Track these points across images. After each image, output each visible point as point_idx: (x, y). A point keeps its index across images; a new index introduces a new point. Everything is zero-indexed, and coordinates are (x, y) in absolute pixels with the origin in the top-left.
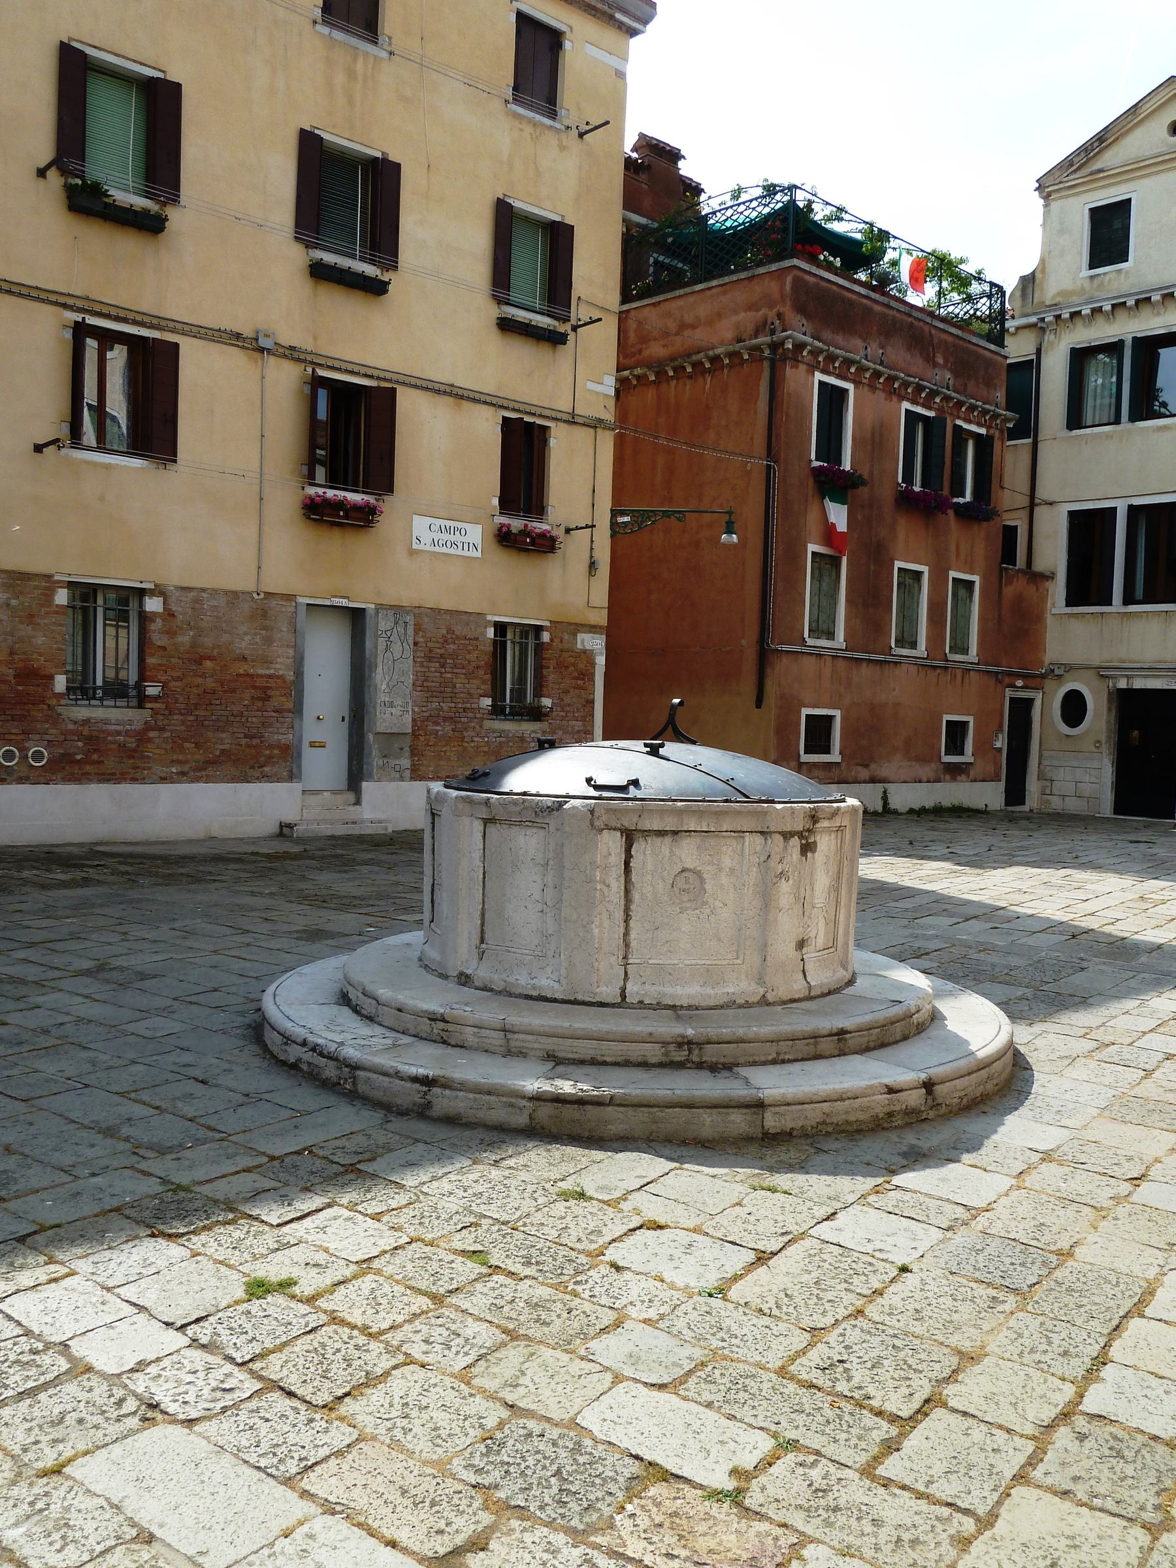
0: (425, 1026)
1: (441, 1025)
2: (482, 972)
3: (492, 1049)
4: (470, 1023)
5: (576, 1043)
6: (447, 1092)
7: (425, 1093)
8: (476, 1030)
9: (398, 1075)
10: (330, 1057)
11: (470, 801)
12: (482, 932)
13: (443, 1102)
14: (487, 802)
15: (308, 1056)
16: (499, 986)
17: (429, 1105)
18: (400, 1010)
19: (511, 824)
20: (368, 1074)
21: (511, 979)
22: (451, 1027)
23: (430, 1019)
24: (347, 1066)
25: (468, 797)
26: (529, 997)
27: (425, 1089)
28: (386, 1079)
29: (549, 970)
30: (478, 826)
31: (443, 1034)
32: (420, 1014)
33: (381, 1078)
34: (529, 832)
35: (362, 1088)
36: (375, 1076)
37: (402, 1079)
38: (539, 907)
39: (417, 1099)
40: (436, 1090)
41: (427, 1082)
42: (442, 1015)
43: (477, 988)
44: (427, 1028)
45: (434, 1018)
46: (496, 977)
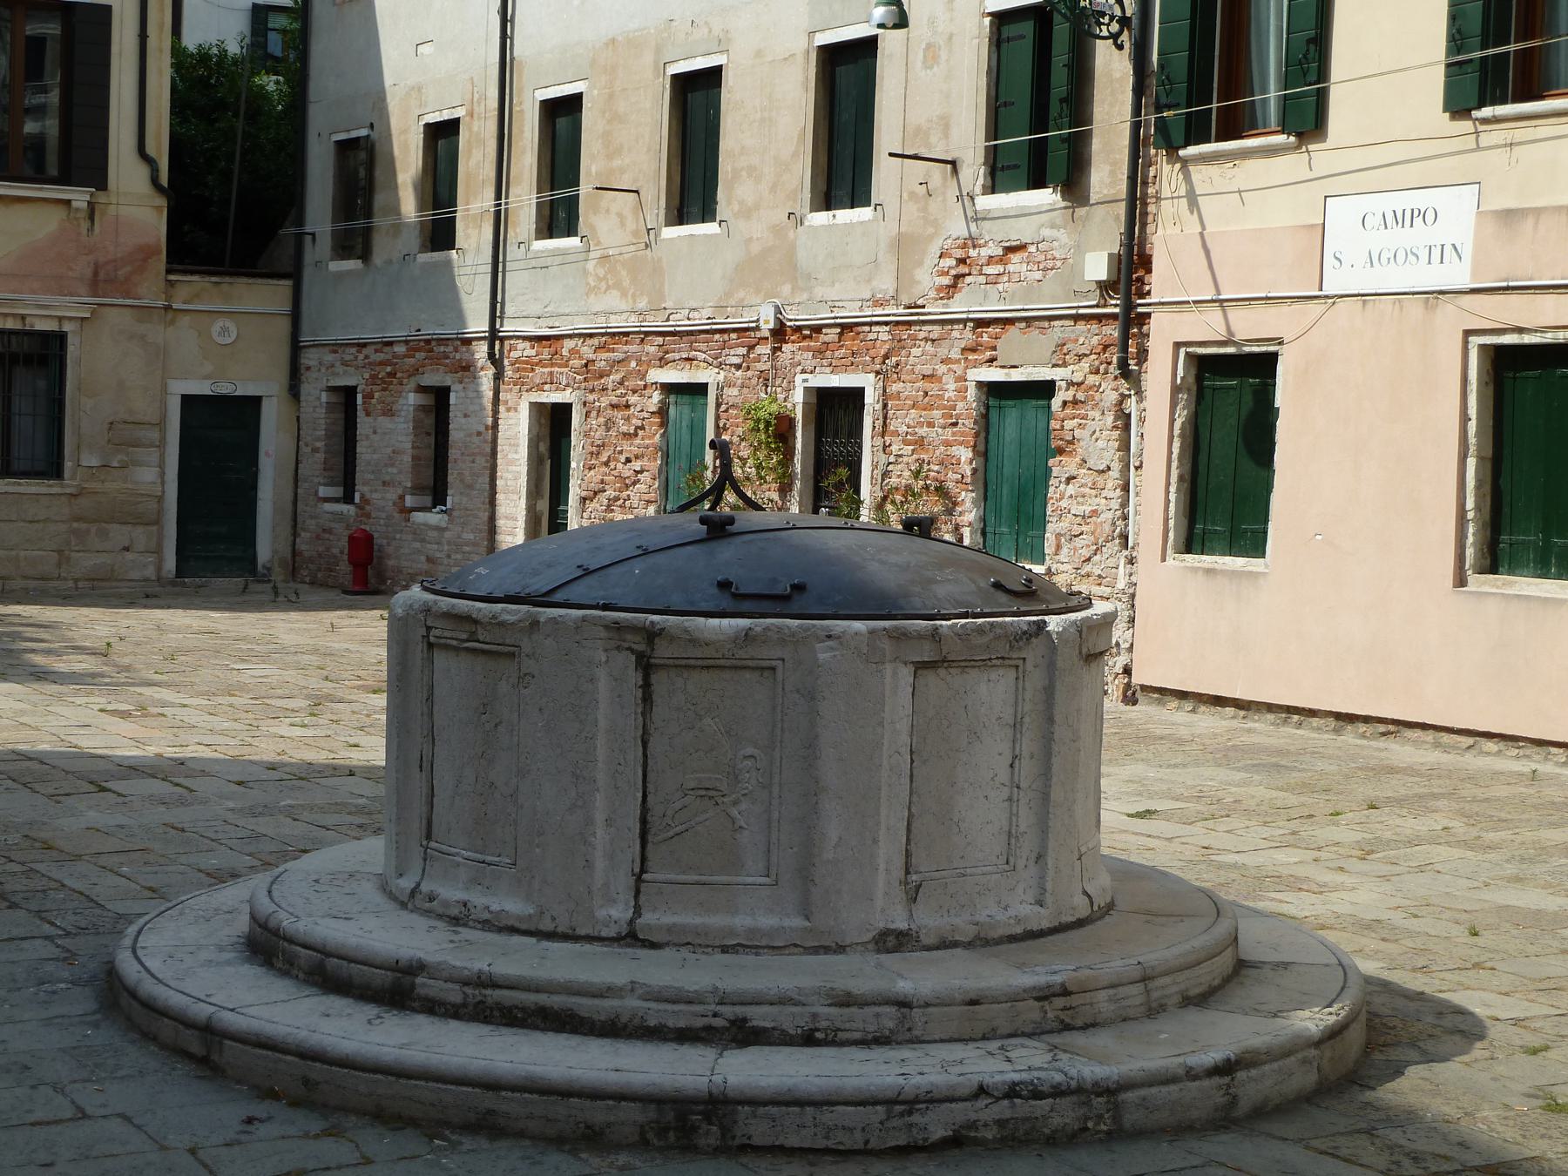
0: (1031, 1011)
1: (1060, 1002)
2: (929, 920)
3: (1131, 1013)
4: (1105, 983)
5: (1198, 971)
6: (1253, 1072)
7: (1229, 1086)
8: (1111, 992)
9: (1191, 1074)
10: (1058, 1092)
11: (900, 637)
12: (908, 854)
13: (1253, 1087)
14: (935, 634)
15: (1002, 1109)
16: (968, 933)
17: (1234, 1101)
18: (973, 1002)
19: (966, 665)
20: (1143, 1092)
21: (981, 917)
22: (1074, 1000)
23: (1038, 999)
24: (1099, 1095)
25: (896, 628)
26: (1013, 939)
27: (1227, 1079)
28: (1173, 1088)
29: (1020, 890)
30: (906, 674)
31: (1062, 1015)
32: (1015, 998)
33: (1164, 1089)
34: (994, 675)
35: (1130, 1118)
36: (1154, 1090)
37: (1196, 1078)
38: (1005, 792)
39: (1220, 1099)
40: (1241, 1075)
41: (1226, 1069)
42: (1063, 985)
43: (929, 948)
44: (1037, 1016)
45: (1044, 995)
46: (957, 921)
